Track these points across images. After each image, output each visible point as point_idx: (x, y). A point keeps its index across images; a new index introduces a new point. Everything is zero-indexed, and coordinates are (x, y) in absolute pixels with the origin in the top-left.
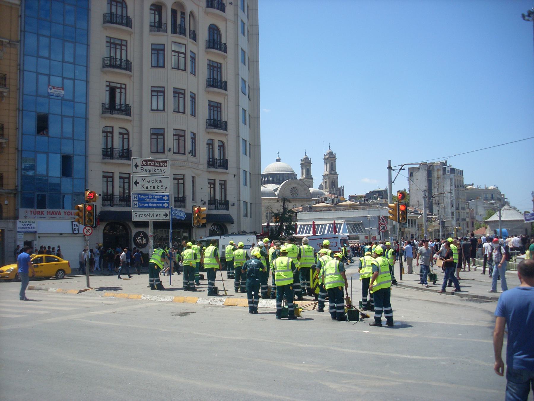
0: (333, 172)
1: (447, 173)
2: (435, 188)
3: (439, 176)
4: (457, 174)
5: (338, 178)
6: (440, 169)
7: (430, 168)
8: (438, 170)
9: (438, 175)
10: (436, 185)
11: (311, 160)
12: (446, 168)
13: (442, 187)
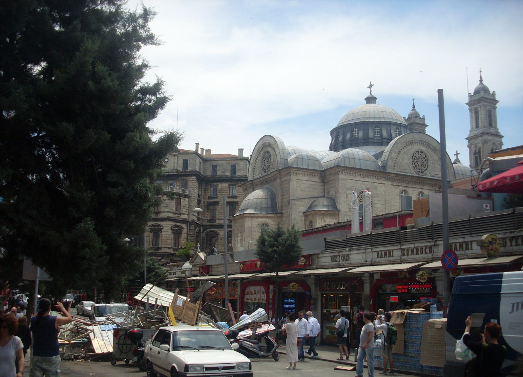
11: (424, 119)
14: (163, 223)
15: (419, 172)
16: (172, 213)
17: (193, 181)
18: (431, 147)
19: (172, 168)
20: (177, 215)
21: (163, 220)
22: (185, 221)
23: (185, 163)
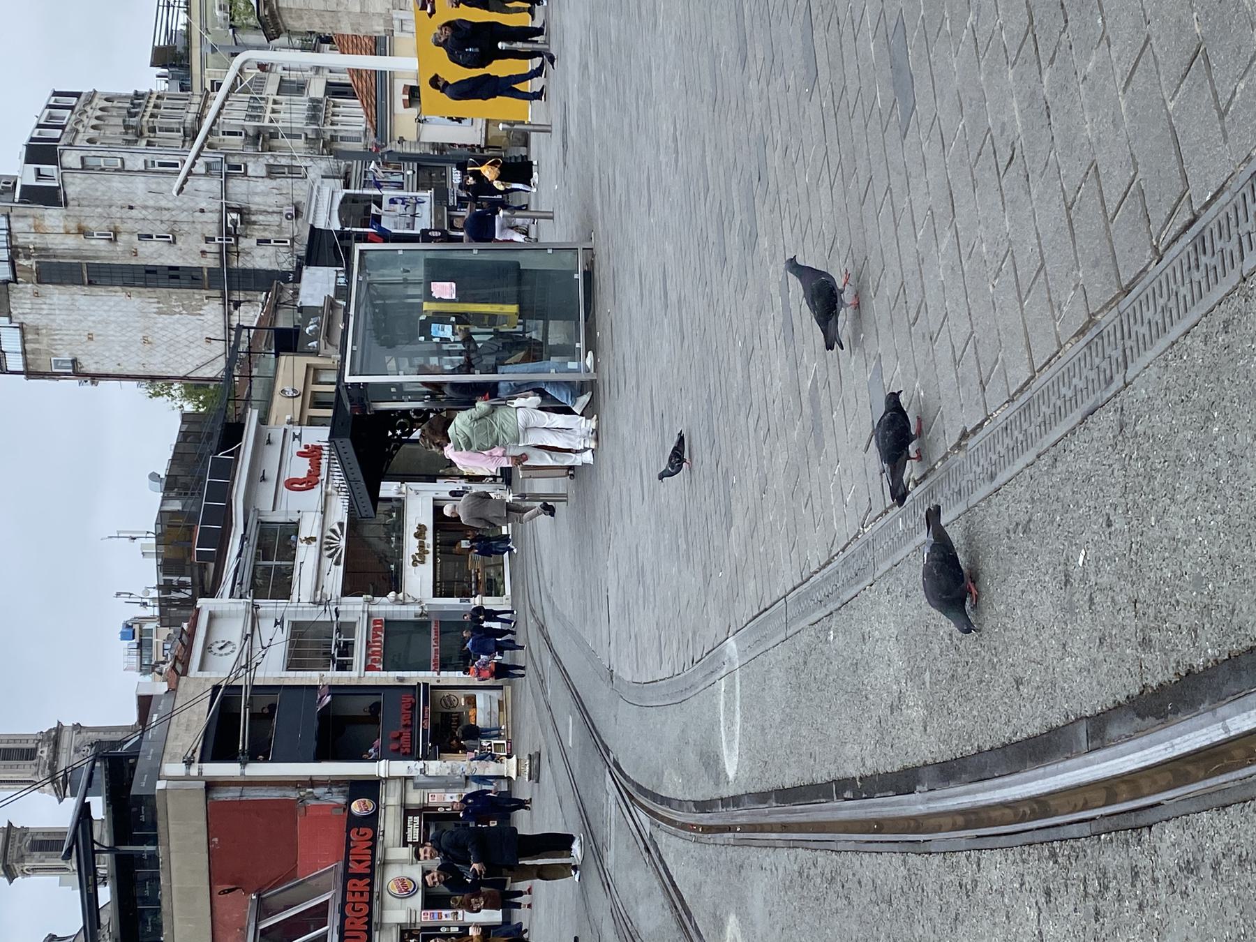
0: (44, 752)
3: (73, 225)
4: (63, 127)
5: (78, 728)
8: (38, 230)
9: (68, 233)
10: (120, 246)
12: (23, 187)
13: (133, 213)
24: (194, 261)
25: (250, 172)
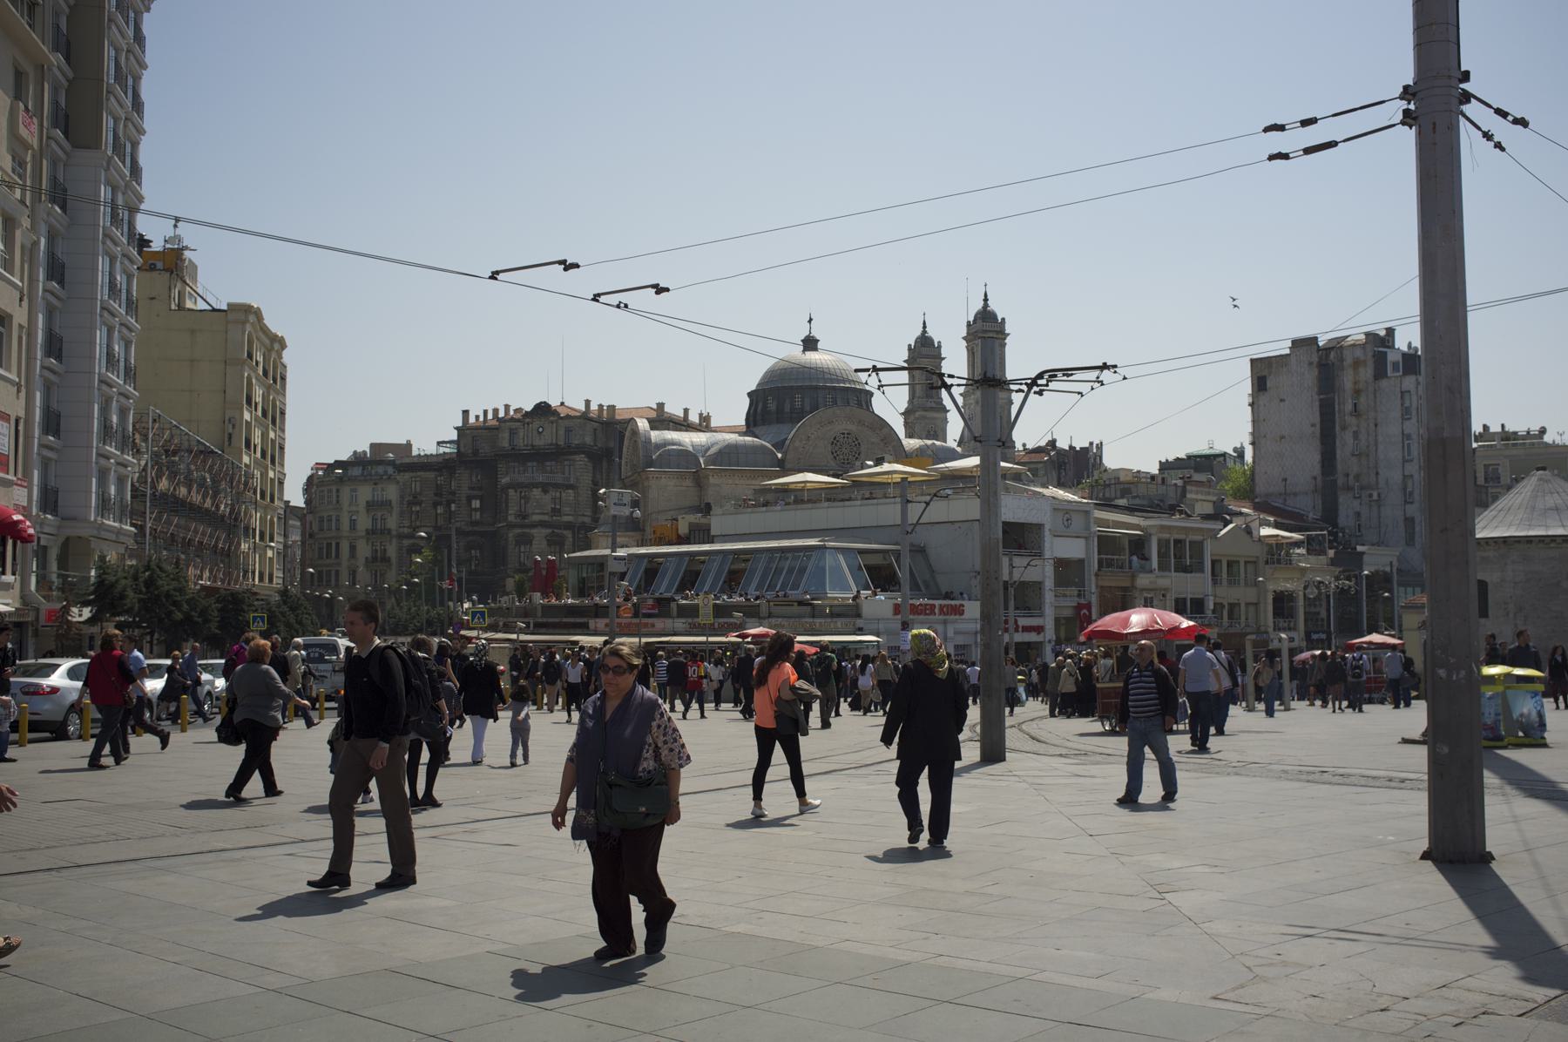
1: (1389, 375)
2: (1344, 428)
6: (1365, 361)
7: (1327, 356)
9: (1355, 383)
11: (939, 347)
12: (1386, 353)
13: (1372, 425)
14: (534, 531)
15: (843, 463)
16: (547, 514)
17: (581, 460)
18: (866, 424)
19: (550, 442)
20: (554, 518)
21: (533, 526)
22: (569, 526)
23: (568, 430)
24: (1339, 467)
25: (1408, 506)
